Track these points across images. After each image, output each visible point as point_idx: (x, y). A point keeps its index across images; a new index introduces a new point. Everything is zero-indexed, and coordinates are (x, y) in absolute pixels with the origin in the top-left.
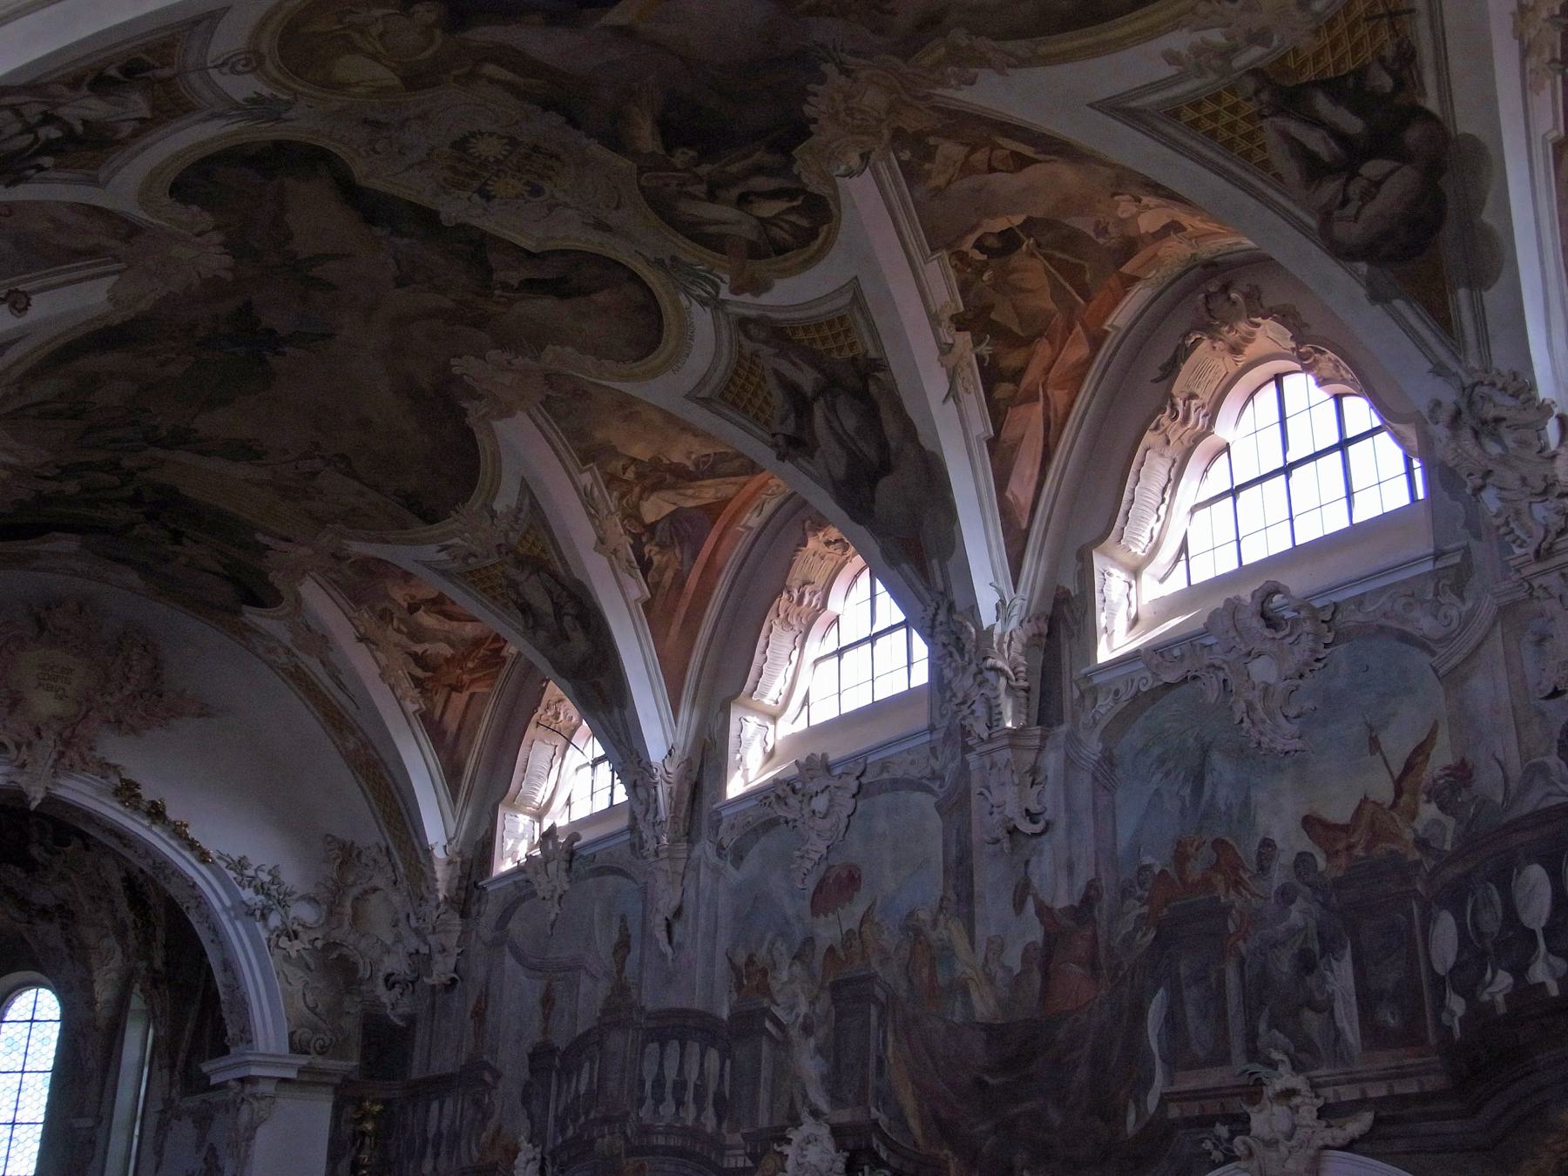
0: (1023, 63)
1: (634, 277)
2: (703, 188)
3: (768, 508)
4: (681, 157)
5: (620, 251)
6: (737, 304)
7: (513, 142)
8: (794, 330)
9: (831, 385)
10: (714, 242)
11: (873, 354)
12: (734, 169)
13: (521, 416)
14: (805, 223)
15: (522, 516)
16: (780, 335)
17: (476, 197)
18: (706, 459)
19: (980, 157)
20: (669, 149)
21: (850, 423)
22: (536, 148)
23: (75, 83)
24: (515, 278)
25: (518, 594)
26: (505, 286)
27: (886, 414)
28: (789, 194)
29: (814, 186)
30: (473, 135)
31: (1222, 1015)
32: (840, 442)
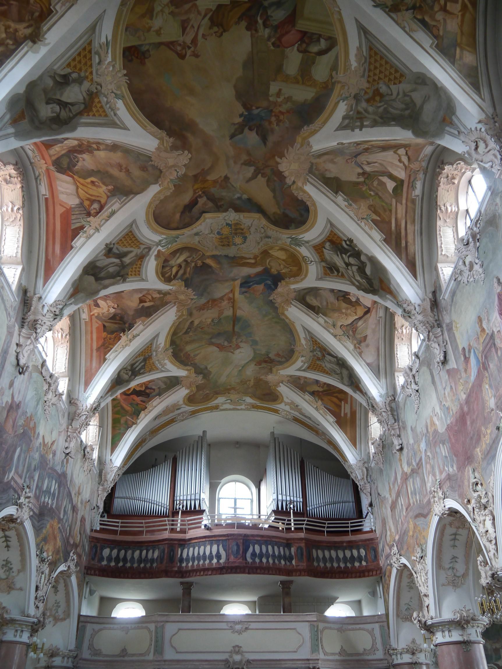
0: (173, 324)
1: (177, 229)
2: (189, 261)
3: (30, 153)
4: (199, 263)
5: (187, 232)
6: (155, 250)
7: (235, 244)
8: (142, 261)
9: (123, 266)
10: (174, 253)
11: (127, 280)
12: (189, 269)
13: (153, 150)
14: (167, 275)
15: (112, 113)
16: (141, 258)
17: (230, 223)
18: (76, 160)
19: (150, 297)
20: (203, 263)
21: (111, 270)
22: (228, 245)
23: (343, 276)
24: (202, 201)
25: (75, 81)
26: (200, 196)
27: (112, 281)
28: (175, 276)
29: (174, 282)
30: (245, 242)
31: (24, 466)
32: (107, 265)
